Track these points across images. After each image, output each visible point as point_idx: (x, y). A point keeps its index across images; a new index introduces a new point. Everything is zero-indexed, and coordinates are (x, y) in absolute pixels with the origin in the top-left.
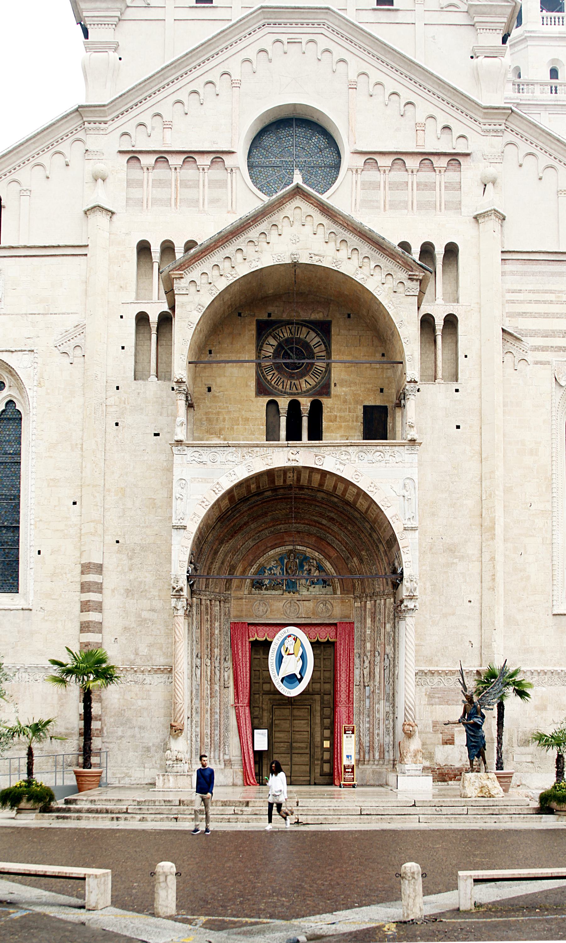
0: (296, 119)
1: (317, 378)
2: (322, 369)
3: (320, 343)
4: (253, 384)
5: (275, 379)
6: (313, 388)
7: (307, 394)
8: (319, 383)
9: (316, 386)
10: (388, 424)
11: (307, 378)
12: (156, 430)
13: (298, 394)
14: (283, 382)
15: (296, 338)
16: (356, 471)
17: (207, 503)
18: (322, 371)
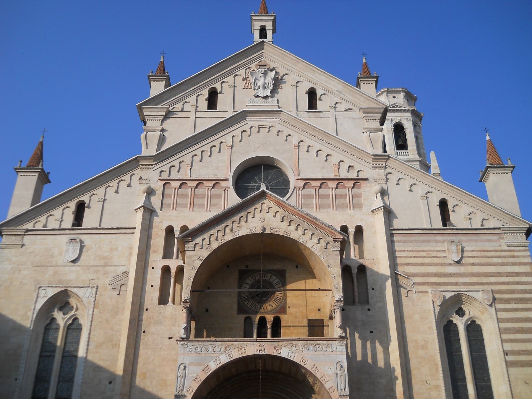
0: (264, 165)
1: (278, 303)
2: (280, 297)
3: (279, 283)
4: (235, 307)
5: (250, 304)
6: (275, 309)
7: (271, 312)
8: (279, 306)
9: (277, 307)
10: (325, 330)
11: (271, 303)
12: (170, 336)
13: (265, 312)
14: (255, 305)
15: (263, 280)
16: (303, 358)
17: (199, 379)
18: (280, 299)
